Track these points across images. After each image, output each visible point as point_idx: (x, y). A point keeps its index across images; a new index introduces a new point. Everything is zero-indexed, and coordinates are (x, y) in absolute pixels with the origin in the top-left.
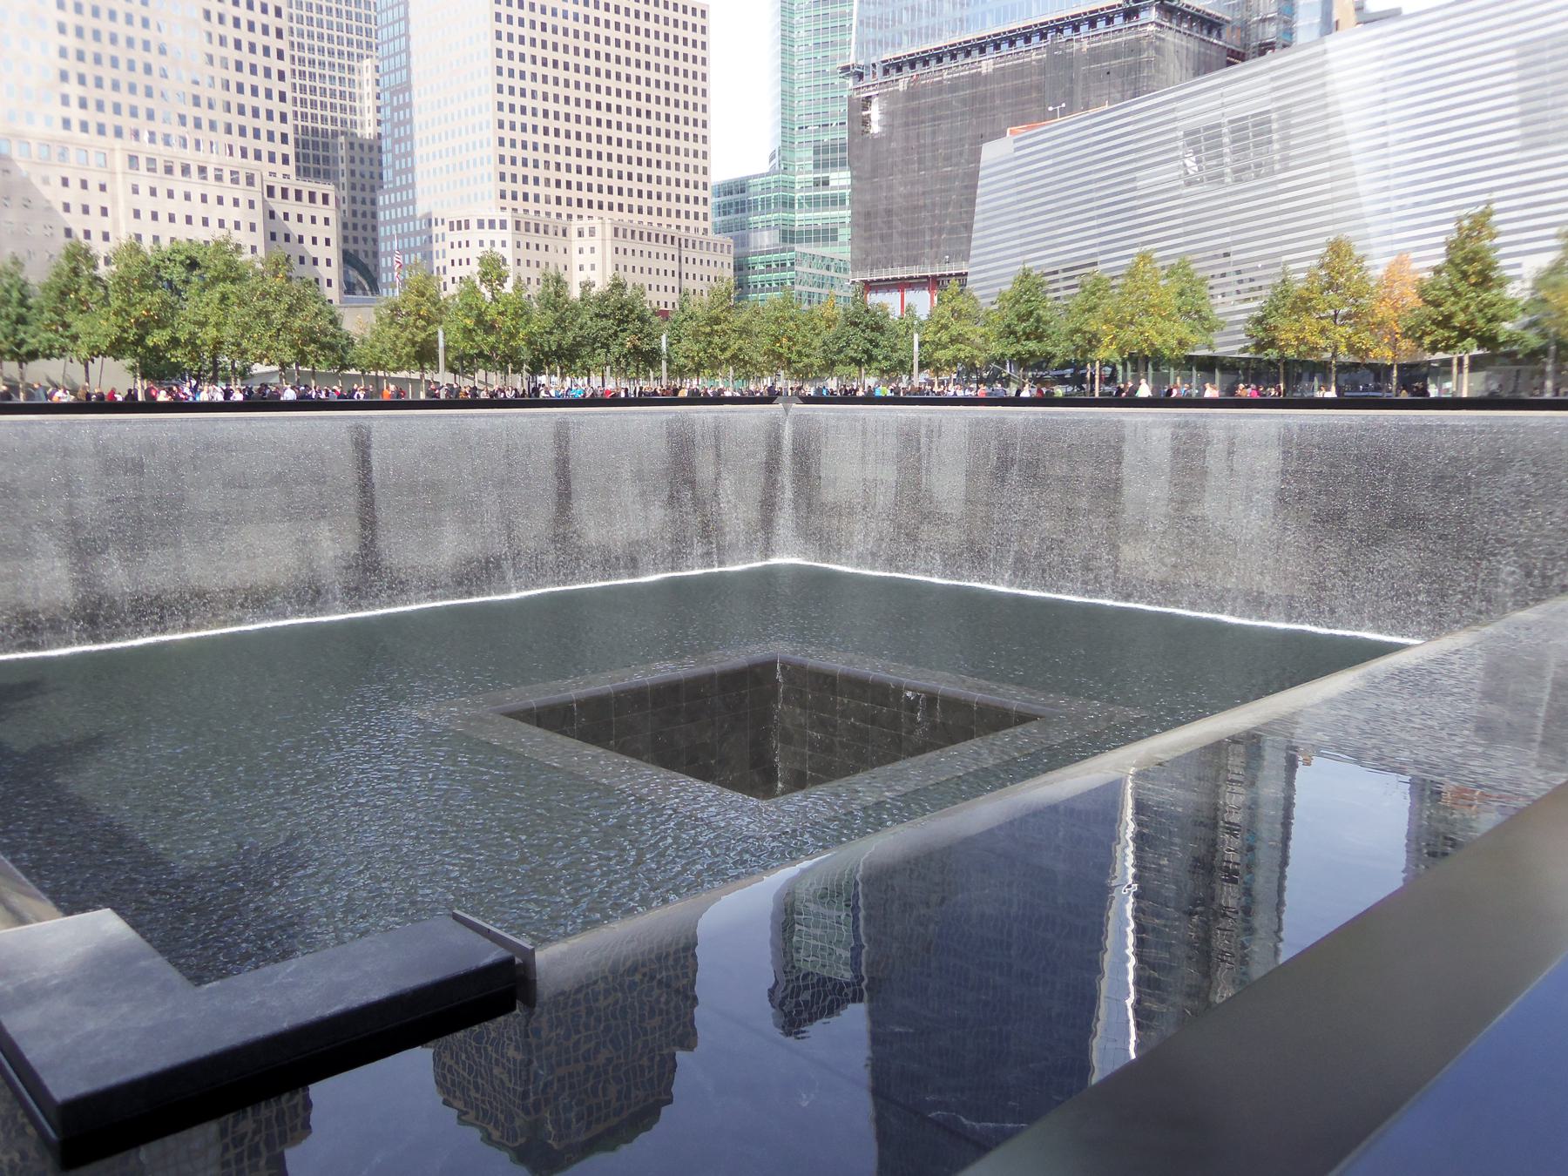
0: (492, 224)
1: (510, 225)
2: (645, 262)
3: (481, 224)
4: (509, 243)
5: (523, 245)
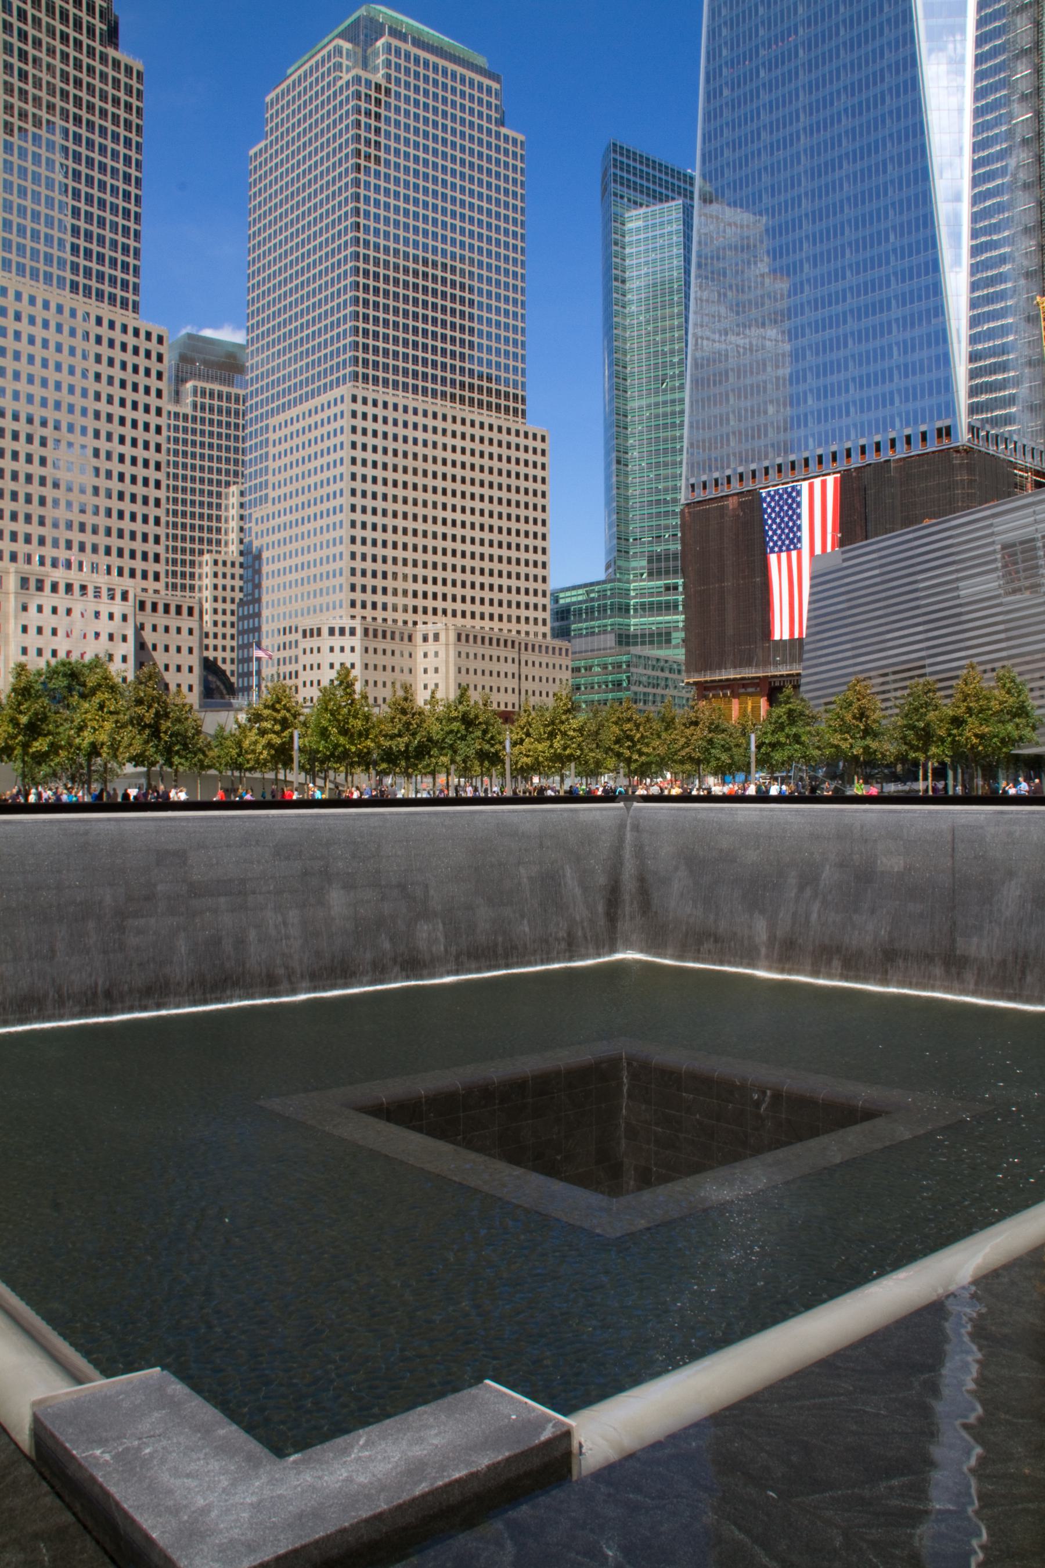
0: (342, 632)
1: (359, 632)
2: (487, 665)
3: (332, 632)
4: (358, 649)
5: (371, 650)
